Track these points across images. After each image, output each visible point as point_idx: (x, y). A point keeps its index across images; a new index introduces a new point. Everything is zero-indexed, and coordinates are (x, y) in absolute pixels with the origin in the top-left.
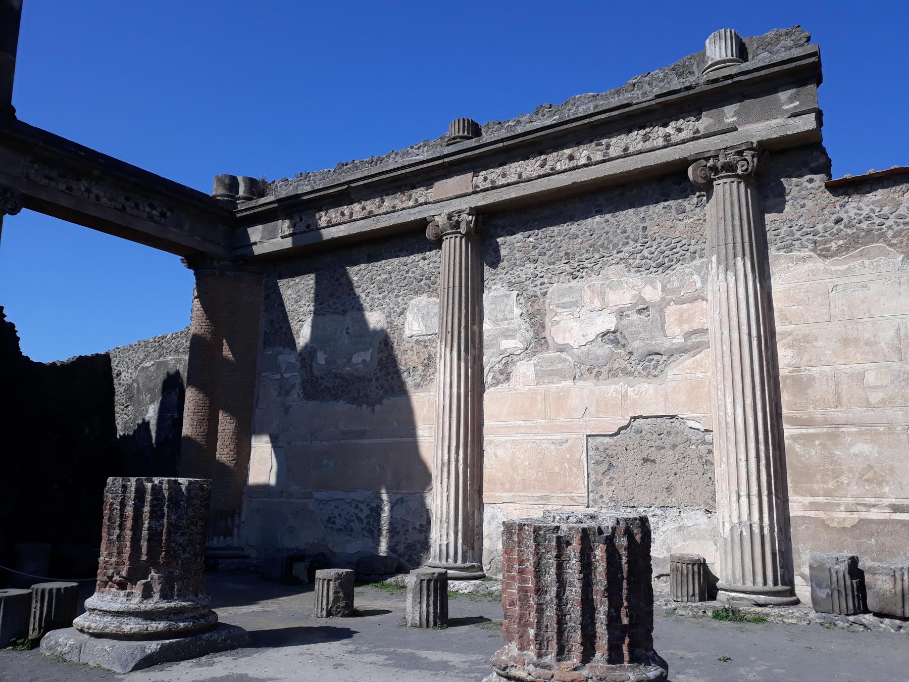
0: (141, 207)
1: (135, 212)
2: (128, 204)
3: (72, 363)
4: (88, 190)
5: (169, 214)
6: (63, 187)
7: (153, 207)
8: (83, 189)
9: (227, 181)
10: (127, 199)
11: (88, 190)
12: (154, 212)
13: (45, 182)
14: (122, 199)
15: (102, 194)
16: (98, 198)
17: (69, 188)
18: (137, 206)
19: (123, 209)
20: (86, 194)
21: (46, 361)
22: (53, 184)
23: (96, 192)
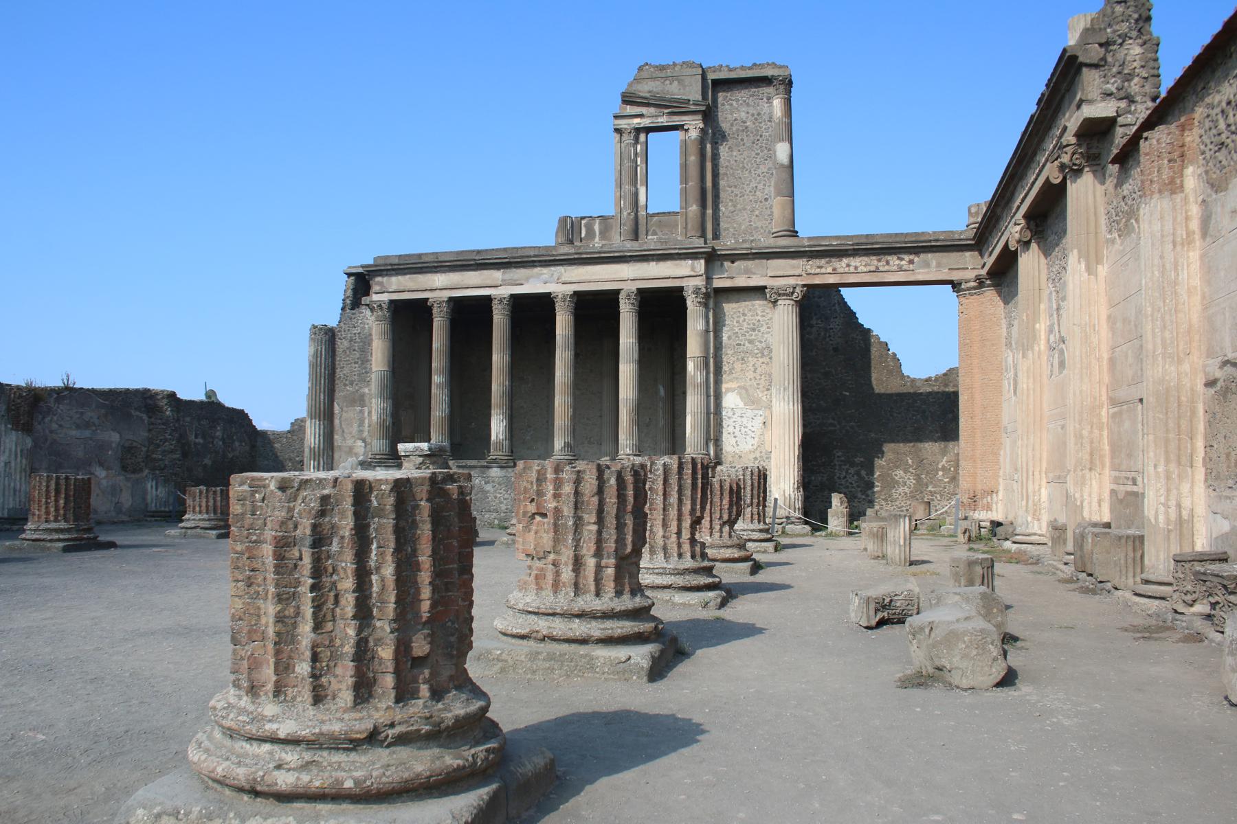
1: (887, 268)
3: (945, 375)
4: (848, 265)
5: (916, 259)
6: (830, 270)
7: (902, 259)
9: (973, 210)
10: (879, 261)
11: (848, 265)
12: (903, 263)
13: (818, 271)
14: (875, 262)
16: (856, 268)
18: (888, 263)
21: (923, 377)
22: (823, 271)
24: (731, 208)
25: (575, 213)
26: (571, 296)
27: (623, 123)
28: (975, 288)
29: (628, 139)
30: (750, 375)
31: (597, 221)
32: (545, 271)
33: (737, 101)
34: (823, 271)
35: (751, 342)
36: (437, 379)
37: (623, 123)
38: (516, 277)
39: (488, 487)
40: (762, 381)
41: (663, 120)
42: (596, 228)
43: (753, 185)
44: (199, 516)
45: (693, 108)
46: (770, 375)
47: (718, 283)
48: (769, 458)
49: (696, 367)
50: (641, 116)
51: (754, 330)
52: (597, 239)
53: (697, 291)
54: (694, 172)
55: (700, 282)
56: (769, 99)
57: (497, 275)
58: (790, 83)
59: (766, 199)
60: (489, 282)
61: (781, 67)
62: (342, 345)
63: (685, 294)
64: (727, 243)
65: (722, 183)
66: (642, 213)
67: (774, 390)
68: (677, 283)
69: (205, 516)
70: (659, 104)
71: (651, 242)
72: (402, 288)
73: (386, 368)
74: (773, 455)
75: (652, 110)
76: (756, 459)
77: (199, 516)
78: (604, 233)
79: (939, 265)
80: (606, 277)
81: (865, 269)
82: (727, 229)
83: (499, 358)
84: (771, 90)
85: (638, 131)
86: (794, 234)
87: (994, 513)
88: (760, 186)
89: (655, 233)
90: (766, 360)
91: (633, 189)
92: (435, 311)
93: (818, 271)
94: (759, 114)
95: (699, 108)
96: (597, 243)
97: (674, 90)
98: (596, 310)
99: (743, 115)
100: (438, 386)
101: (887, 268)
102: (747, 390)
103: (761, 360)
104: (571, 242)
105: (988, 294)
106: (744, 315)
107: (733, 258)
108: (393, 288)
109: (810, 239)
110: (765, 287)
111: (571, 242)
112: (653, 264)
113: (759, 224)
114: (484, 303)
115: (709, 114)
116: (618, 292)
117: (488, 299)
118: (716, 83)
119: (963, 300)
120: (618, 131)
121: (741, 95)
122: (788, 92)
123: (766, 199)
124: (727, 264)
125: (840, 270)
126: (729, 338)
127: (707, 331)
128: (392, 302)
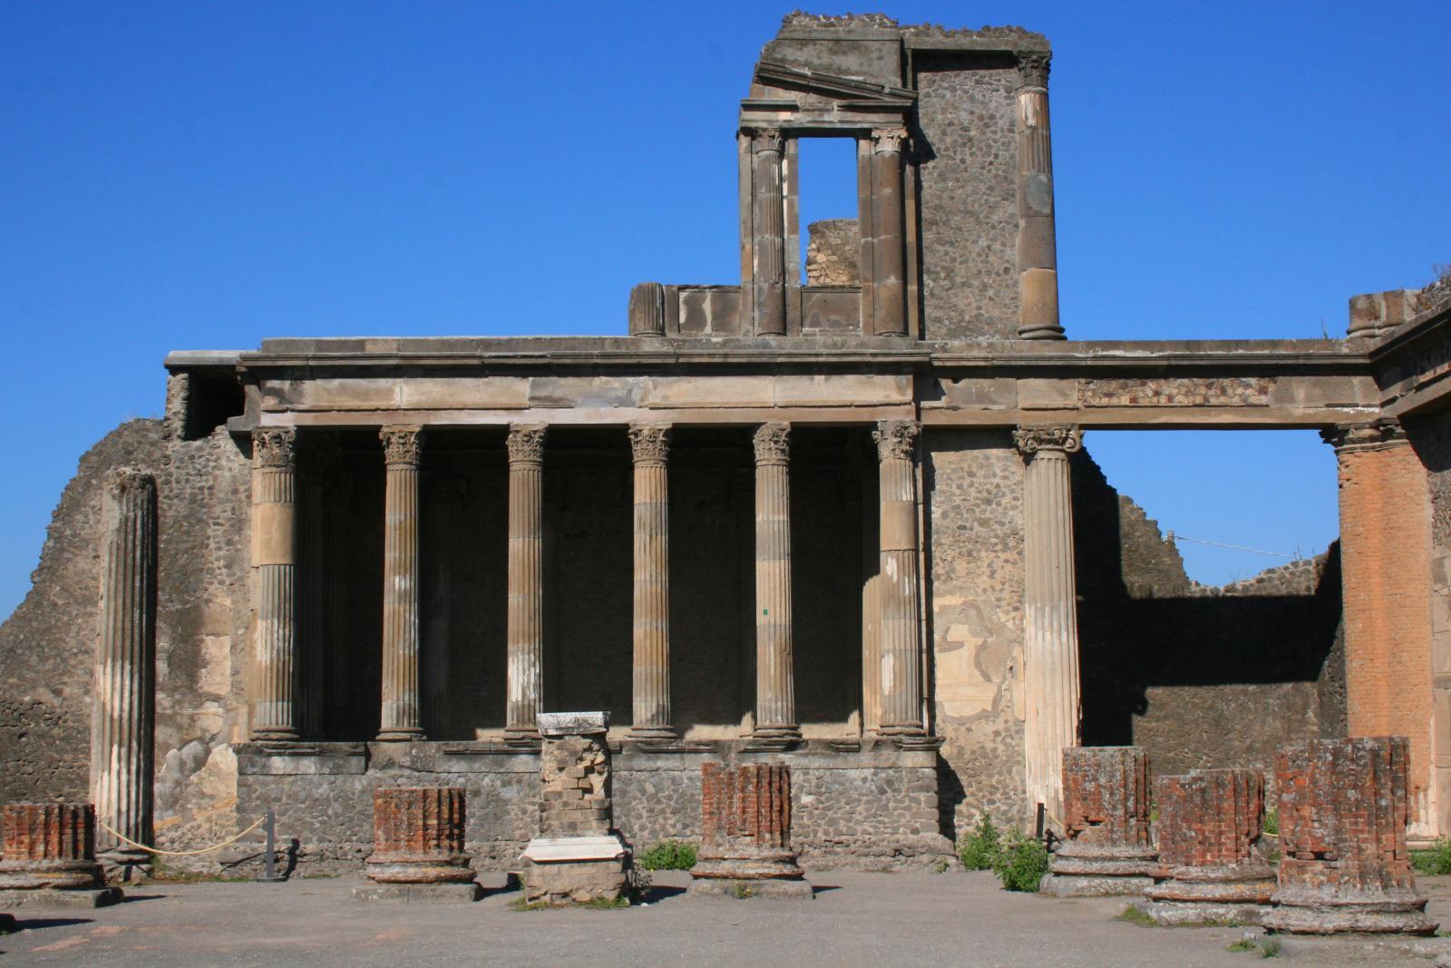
0: (1230, 391)
2: (1212, 392)
5: (1271, 387)
6: (1125, 400)
7: (1248, 386)
8: (1150, 393)
10: (1209, 387)
11: (1157, 393)
12: (1249, 392)
13: (1105, 401)
14: (1203, 390)
15: (1175, 391)
16: (1170, 398)
17: (1133, 400)
18: (1223, 391)
19: (1206, 398)
20: (1155, 400)
22: (1114, 401)
23: (1167, 392)
24: (946, 283)
25: (668, 276)
26: (667, 433)
27: (758, 119)
28: (1372, 439)
29: (767, 148)
30: (984, 581)
31: (709, 295)
32: (617, 384)
33: (953, 89)
34: (1114, 401)
35: (983, 523)
36: (398, 584)
37: (758, 119)
38: (558, 393)
39: (510, 793)
40: (1006, 595)
41: (834, 116)
42: (707, 306)
43: (983, 243)
44: (45, 864)
45: (888, 101)
46: (1021, 582)
47: (929, 419)
48: (1020, 732)
49: (901, 567)
50: (793, 108)
51: (989, 502)
52: (708, 329)
53: (900, 432)
54: (887, 214)
55: (905, 416)
56: (1008, 91)
57: (522, 388)
58: (1047, 69)
59: (1007, 270)
60: (504, 400)
61: (1033, 37)
62: (171, 510)
63: (876, 435)
64: (949, 347)
65: (928, 236)
66: (793, 284)
67: (1029, 611)
68: (864, 416)
69: (58, 862)
70: (825, 87)
71: (816, 340)
72: (324, 404)
73: (288, 560)
74: (1028, 727)
75: (813, 99)
76: (997, 733)
77: (45, 864)
78: (723, 319)
79: (1309, 398)
80: (734, 400)
81: (1186, 402)
82: (938, 320)
83: (522, 548)
84: (1012, 75)
85: (788, 133)
86: (1057, 333)
87: (1422, 825)
88: (997, 246)
89: (815, 324)
90: (1012, 556)
91: (778, 240)
92: (392, 453)
93: (1105, 401)
94: (992, 117)
95: (899, 102)
96: (710, 340)
97: (853, 68)
98: (710, 463)
99: (964, 116)
100: (403, 596)
101: (1223, 400)
102: (979, 610)
103: (1003, 556)
104: (661, 331)
105: (1397, 450)
106: (971, 474)
107: (957, 373)
108: (307, 403)
109: (1091, 345)
110: (1014, 427)
111: (661, 331)
112: (819, 379)
113: (996, 313)
114: (487, 445)
115: (910, 117)
116: (753, 428)
117: (504, 431)
118: (916, 53)
119: (1345, 457)
120: (751, 133)
121: (964, 80)
122: (1044, 80)
123: (1007, 270)
124: (945, 383)
125: (1142, 402)
126: (944, 515)
127: (916, 504)
128: (302, 431)
